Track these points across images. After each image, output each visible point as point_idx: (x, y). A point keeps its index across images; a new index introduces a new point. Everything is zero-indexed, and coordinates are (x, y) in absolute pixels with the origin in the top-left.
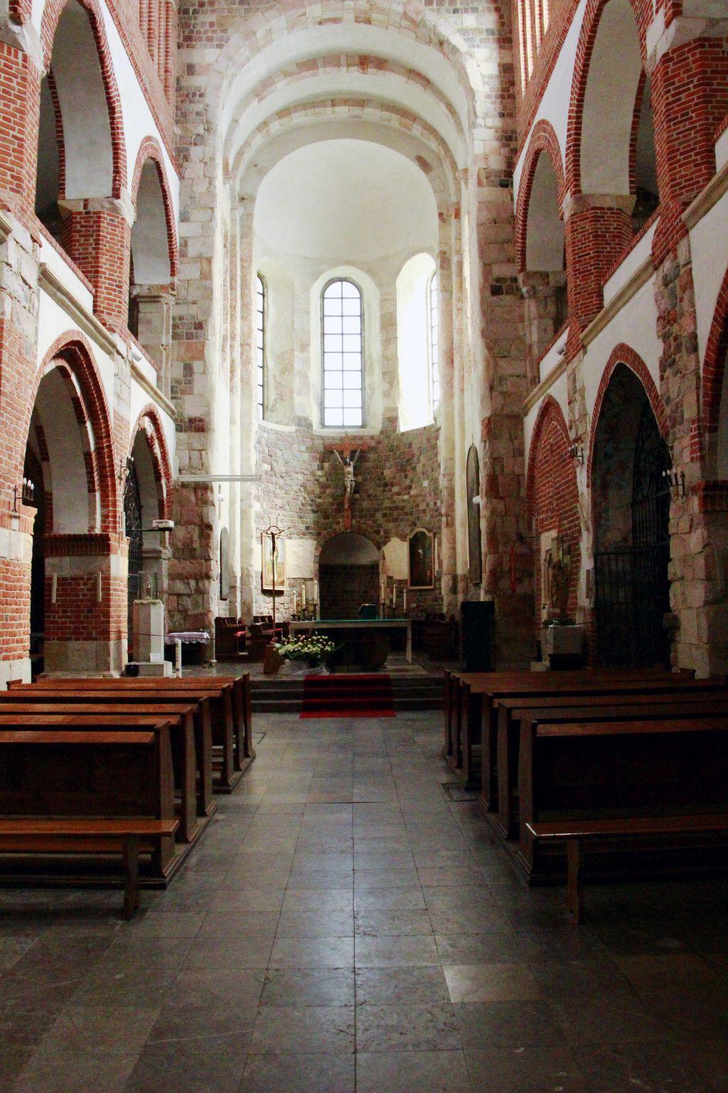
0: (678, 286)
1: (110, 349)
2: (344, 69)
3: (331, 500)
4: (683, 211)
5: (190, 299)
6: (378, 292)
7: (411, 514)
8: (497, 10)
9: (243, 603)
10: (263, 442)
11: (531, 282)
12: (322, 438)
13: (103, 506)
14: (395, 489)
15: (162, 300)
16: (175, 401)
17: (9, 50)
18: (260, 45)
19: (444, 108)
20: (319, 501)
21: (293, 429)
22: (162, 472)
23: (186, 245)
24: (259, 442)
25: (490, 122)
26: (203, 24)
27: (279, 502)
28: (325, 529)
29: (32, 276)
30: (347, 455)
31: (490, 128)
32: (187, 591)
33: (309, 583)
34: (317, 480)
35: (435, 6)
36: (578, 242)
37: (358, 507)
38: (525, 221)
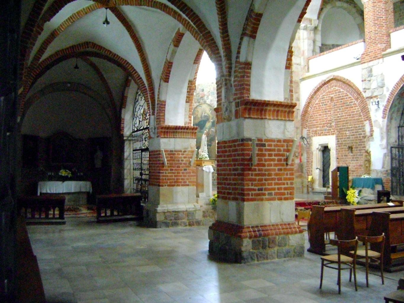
36: (377, 11)
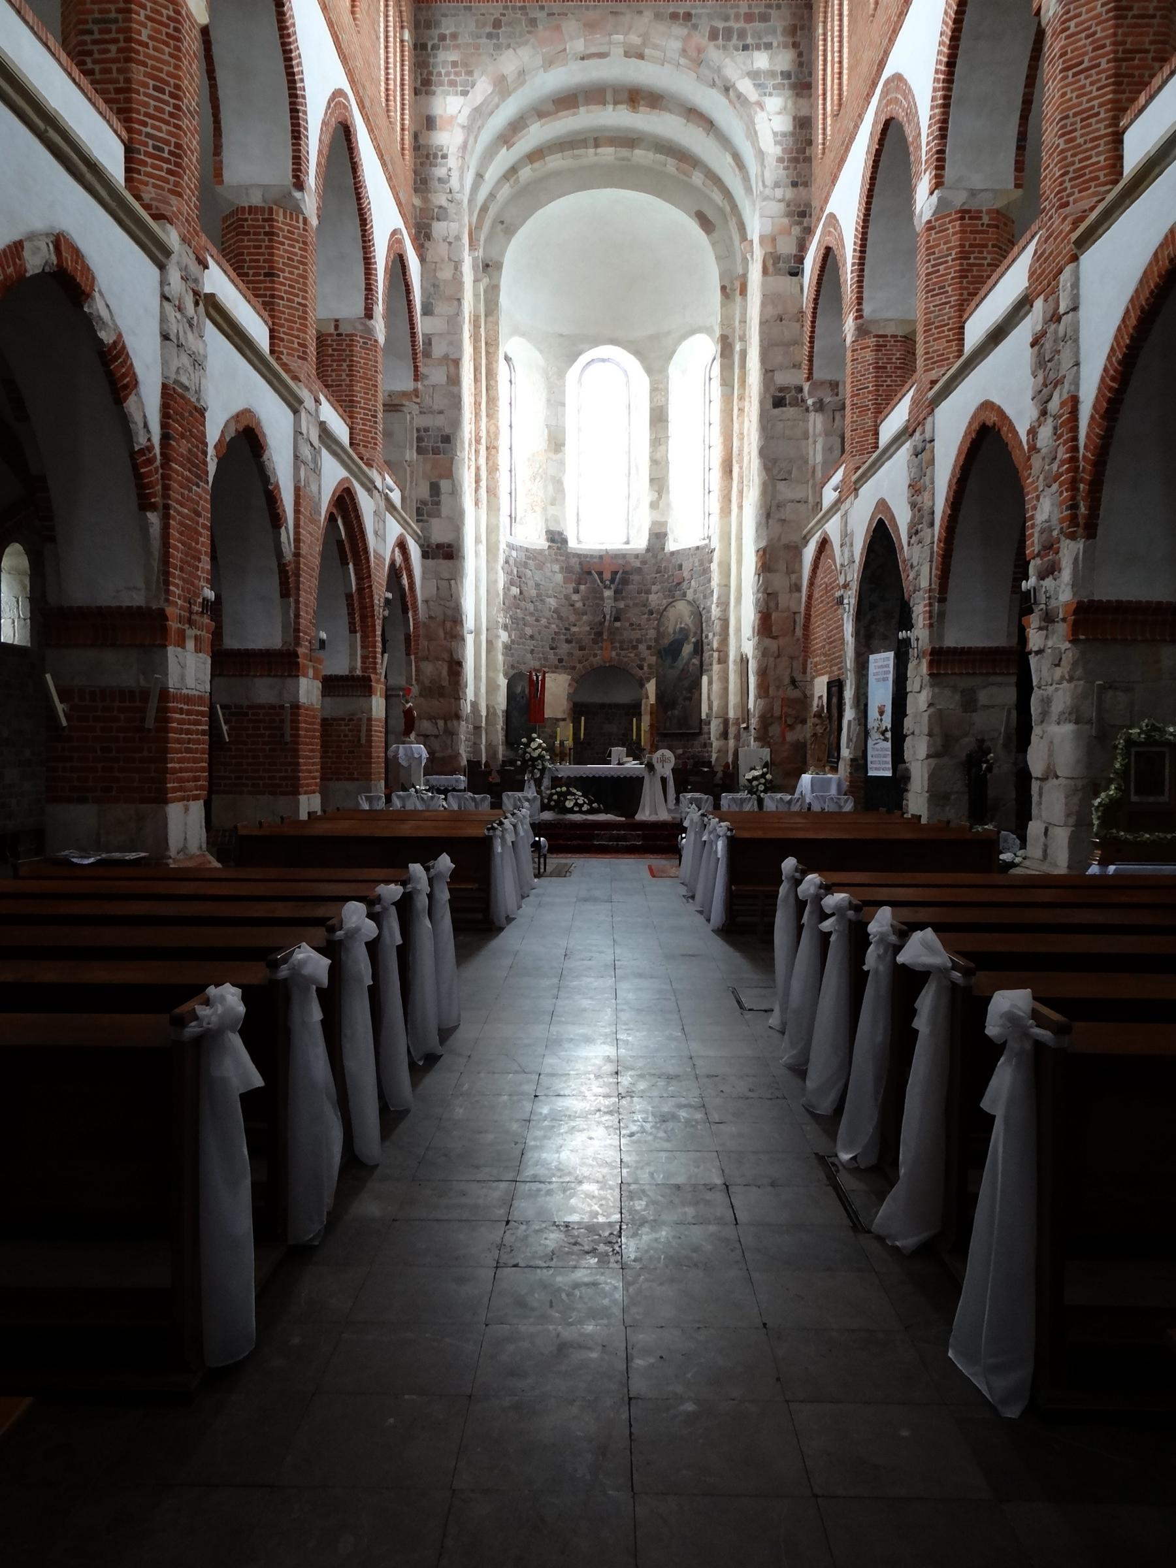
0: (923, 455)
1: (370, 487)
2: (611, 107)
4: (931, 388)
5: (435, 407)
8: (795, 45)
9: (489, 745)
10: (512, 562)
11: (820, 394)
12: (578, 556)
13: (362, 647)
15: (405, 409)
17: (291, 214)
18: (511, 89)
19: (729, 159)
20: (574, 629)
21: (541, 543)
23: (430, 344)
24: (507, 562)
25: (779, 193)
26: (444, 62)
27: (529, 631)
28: (580, 662)
29: (314, 437)
30: (607, 576)
31: (780, 201)
32: (435, 732)
33: (562, 723)
35: (720, 41)
37: (618, 637)
38: (813, 322)
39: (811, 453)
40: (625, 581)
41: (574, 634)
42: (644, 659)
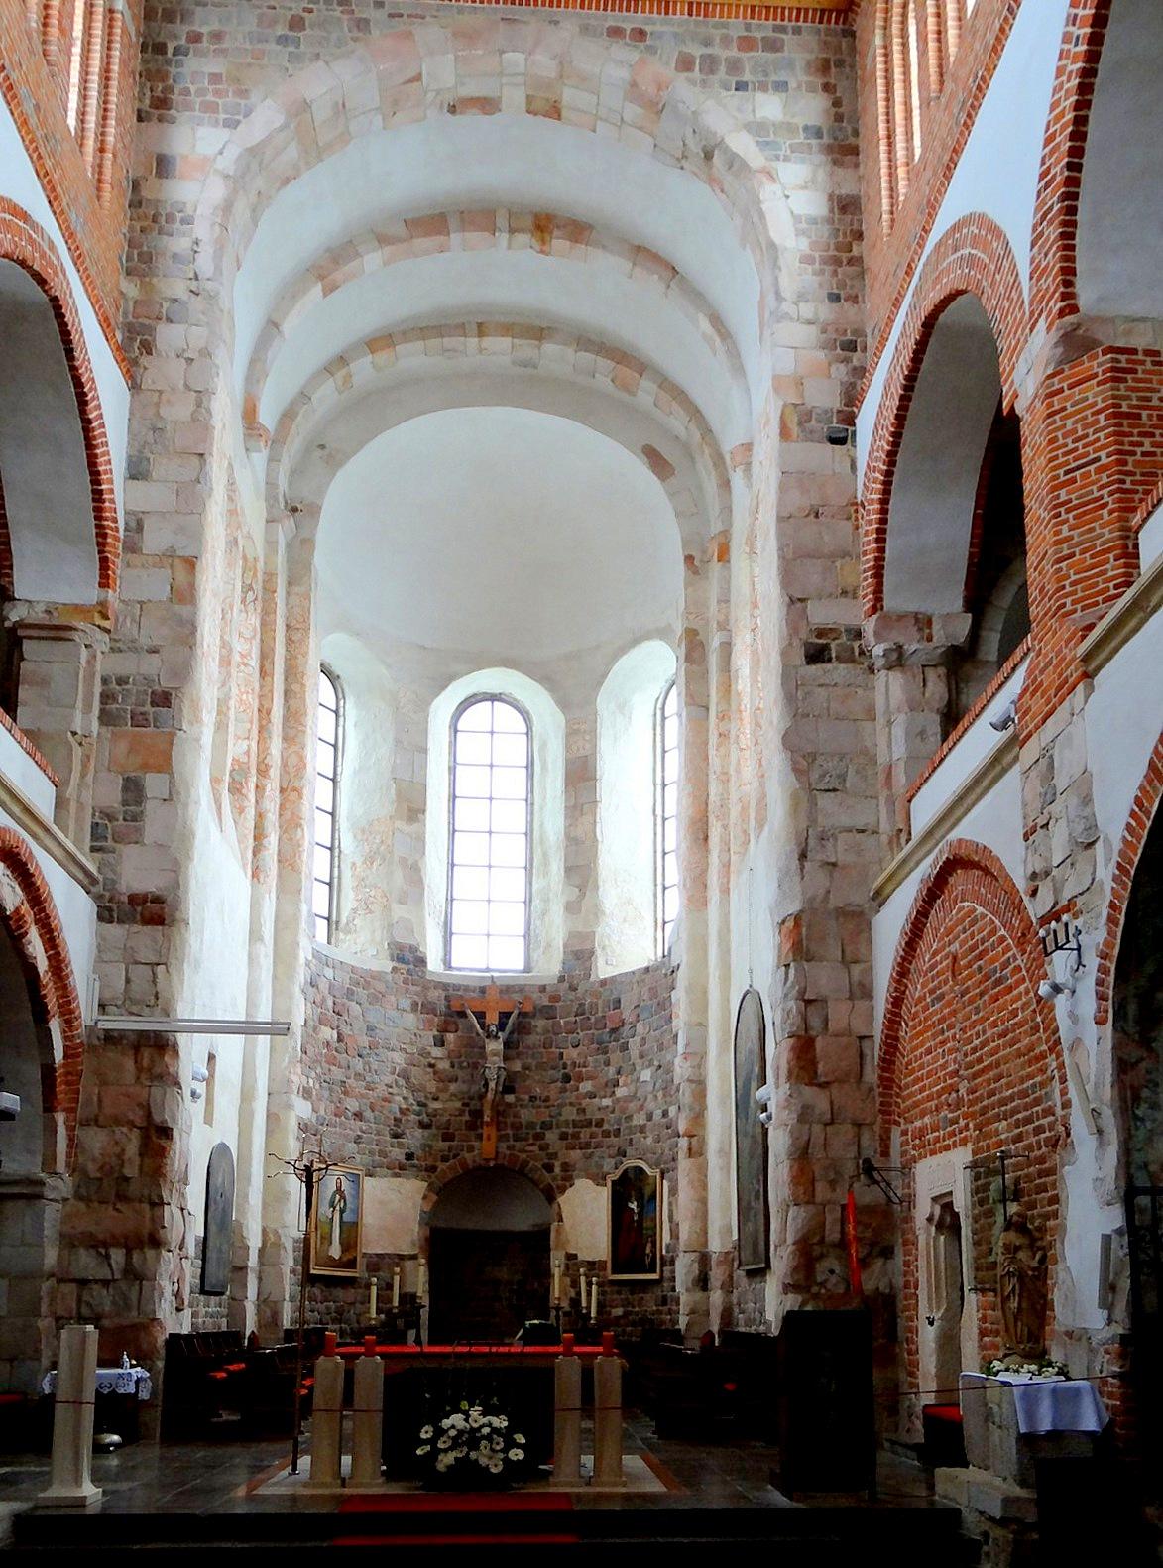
3: (458, 1104)
6: (561, 718)
7: (617, 1133)
10: (324, 985)
12: (445, 986)
14: (586, 1086)
16: (98, 855)
20: (436, 1105)
21: (385, 965)
22: (52, 1003)
27: (352, 1105)
28: (445, 1159)
30: (492, 1018)
33: (409, 1264)
34: (431, 1066)
39: (882, 741)
40: (523, 1028)
41: (435, 1113)
42: (554, 1156)
